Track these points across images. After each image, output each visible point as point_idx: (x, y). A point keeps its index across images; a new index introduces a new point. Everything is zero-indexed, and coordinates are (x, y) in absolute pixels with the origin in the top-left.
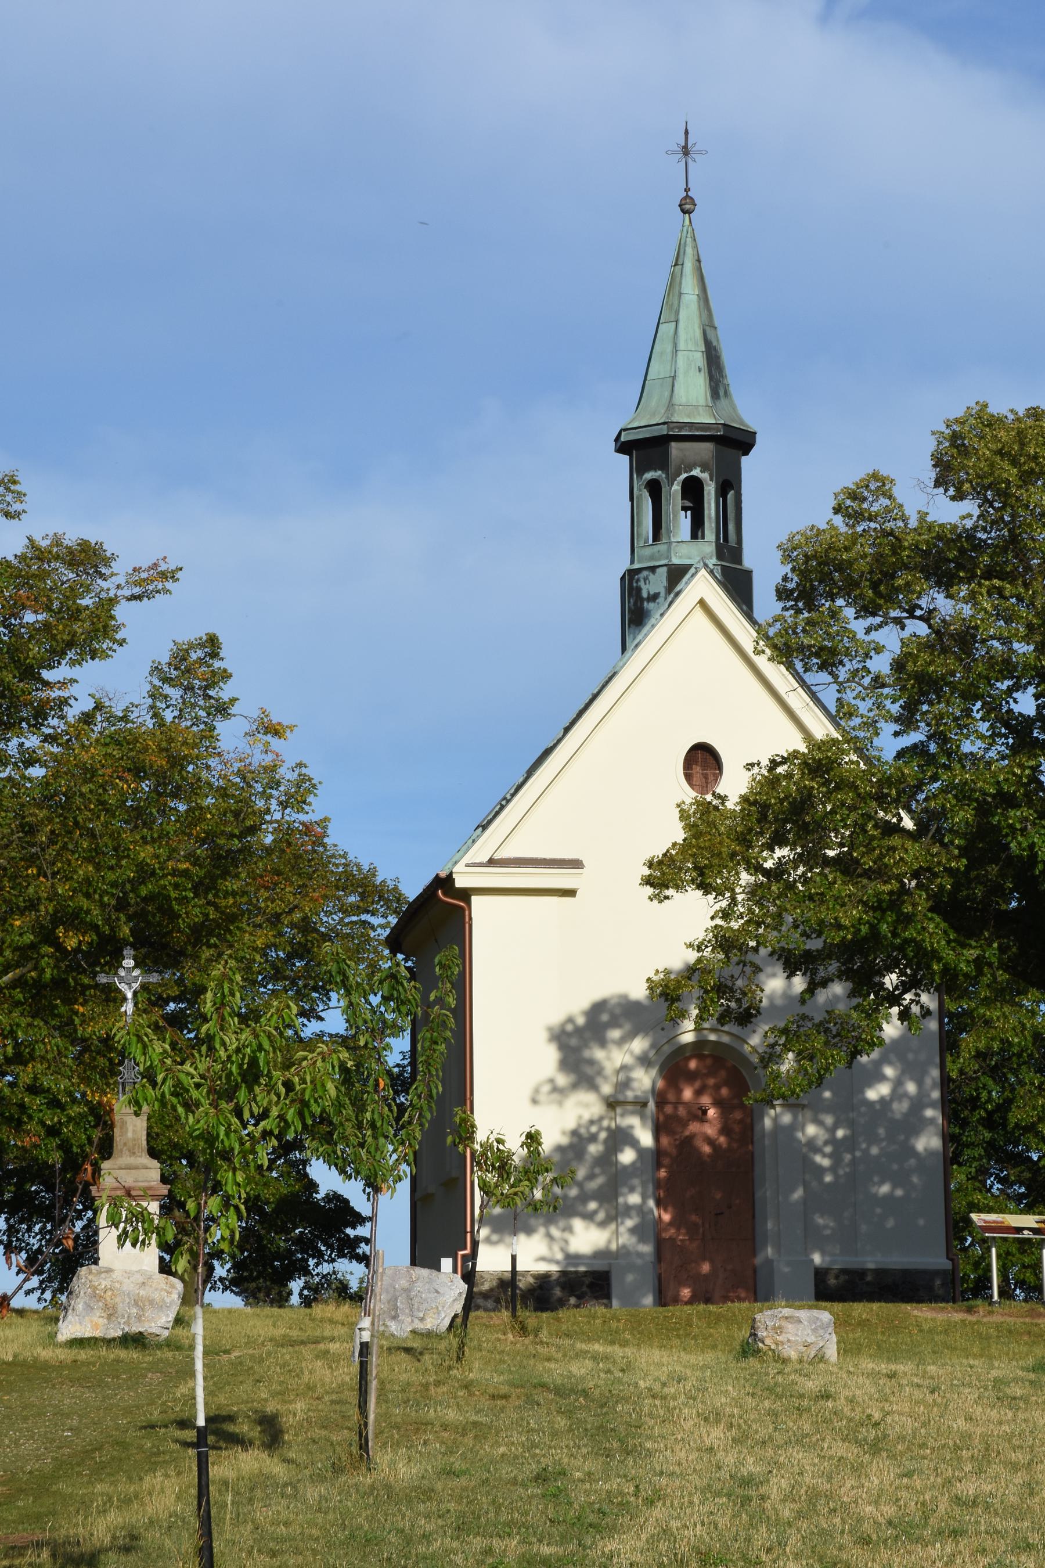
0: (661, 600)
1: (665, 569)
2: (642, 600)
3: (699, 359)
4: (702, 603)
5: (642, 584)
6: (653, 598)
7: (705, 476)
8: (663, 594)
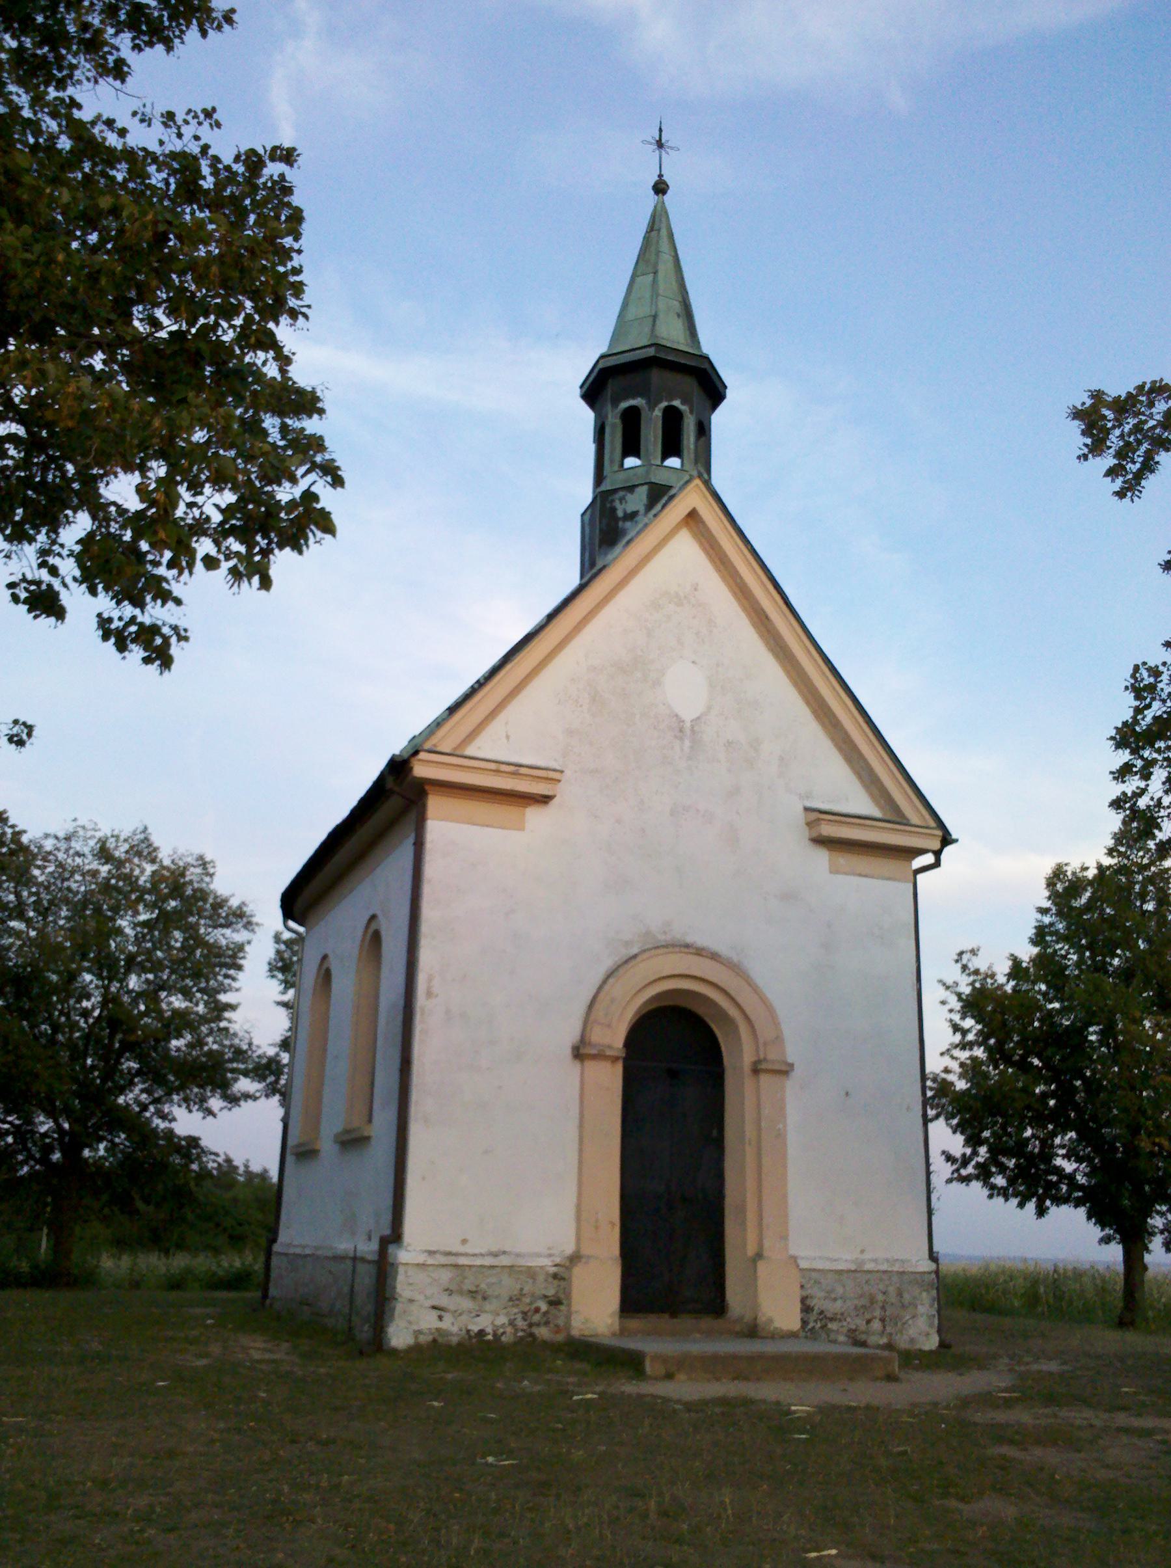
0: (638, 518)
1: (645, 488)
2: (617, 519)
3: (677, 306)
4: (693, 516)
5: (617, 504)
8: (642, 509)
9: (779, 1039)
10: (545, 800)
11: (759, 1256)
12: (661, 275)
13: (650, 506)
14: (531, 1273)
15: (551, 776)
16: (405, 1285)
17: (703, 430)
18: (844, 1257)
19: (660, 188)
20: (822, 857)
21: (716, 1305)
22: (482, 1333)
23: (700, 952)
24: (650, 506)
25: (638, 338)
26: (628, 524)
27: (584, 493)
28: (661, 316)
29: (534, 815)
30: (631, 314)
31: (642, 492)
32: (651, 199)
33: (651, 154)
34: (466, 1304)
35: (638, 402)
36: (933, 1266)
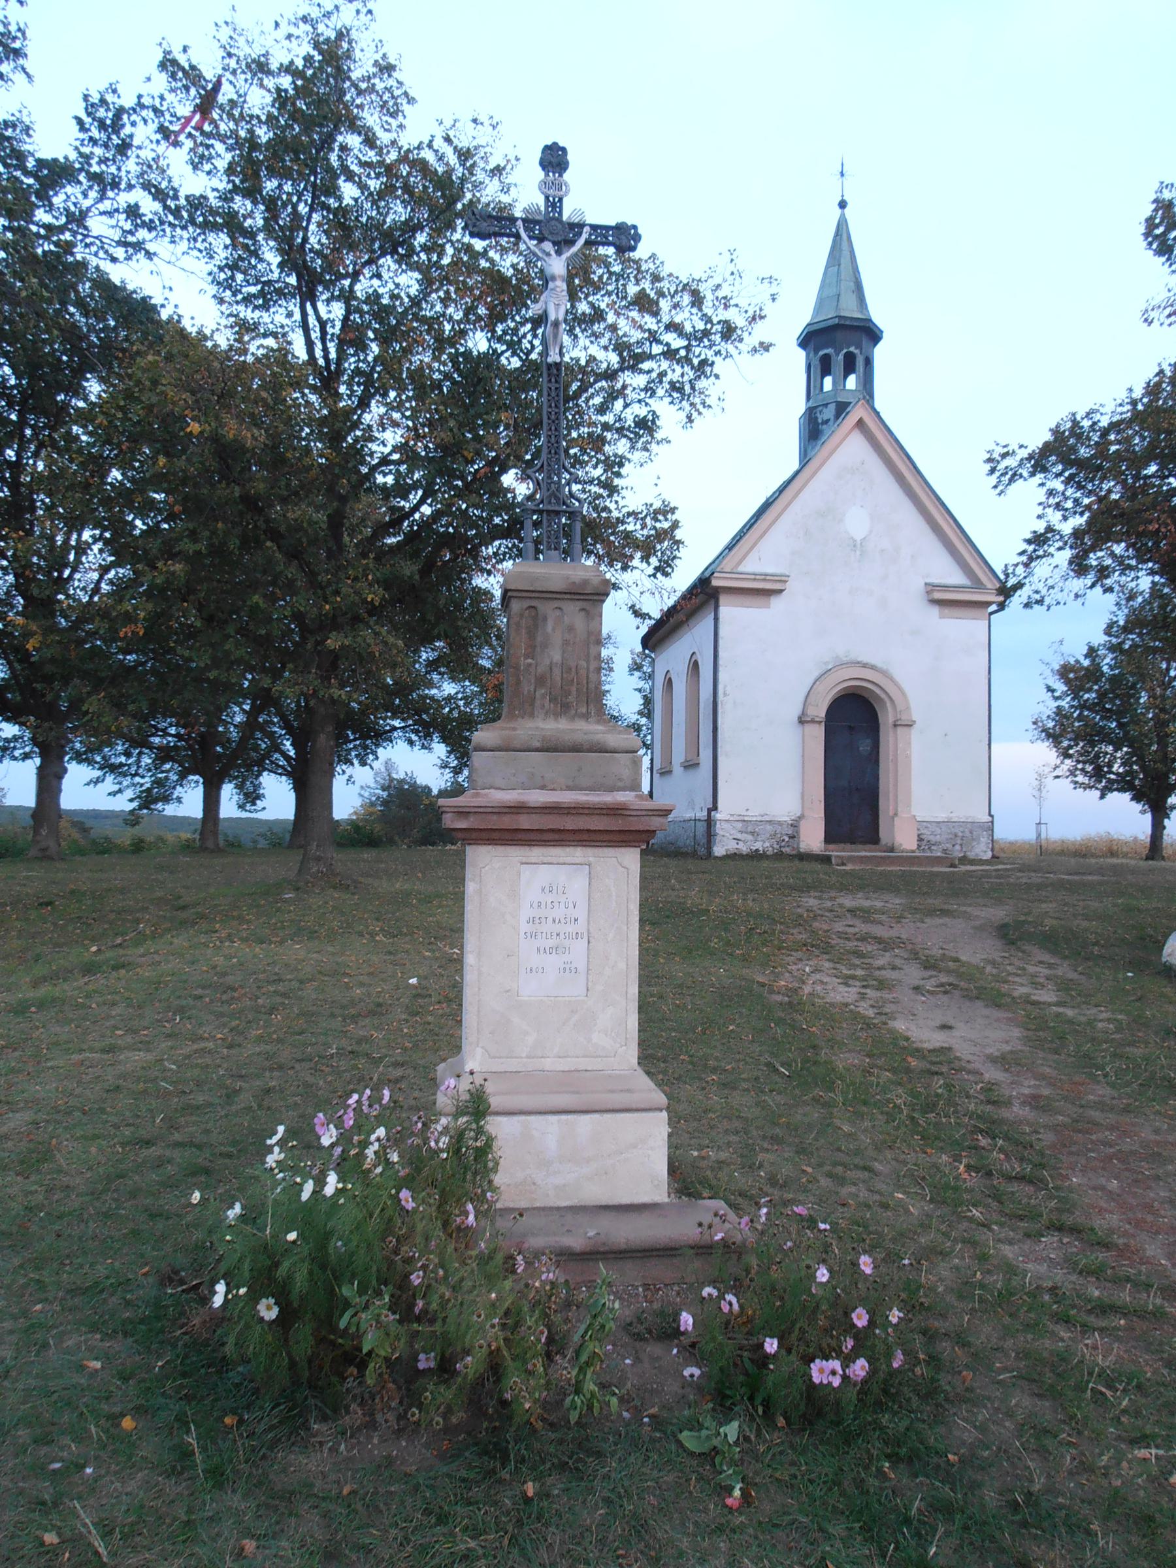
0: (831, 423)
6: (826, 422)
7: (857, 351)
9: (908, 708)
10: (781, 591)
11: (896, 814)
12: (842, 266)
13: (837, 416)
14: (780, 823)
15: (783, 579)
16: (719, 829)
17: (869, 362)
18: (942, 816)
19: (843, 205)
20: (935, 611)
21: (873, 838)
22: (757, 850)
23: (865, 666)
24: (837, 416)
25: (829, 313)
26: (824, 427)
27: (801, 407)
28: (842, 293)
29: (775, 601)
31: (832, 407)
32: (839, 211)
34: (750, 837)
35: (829, 351)
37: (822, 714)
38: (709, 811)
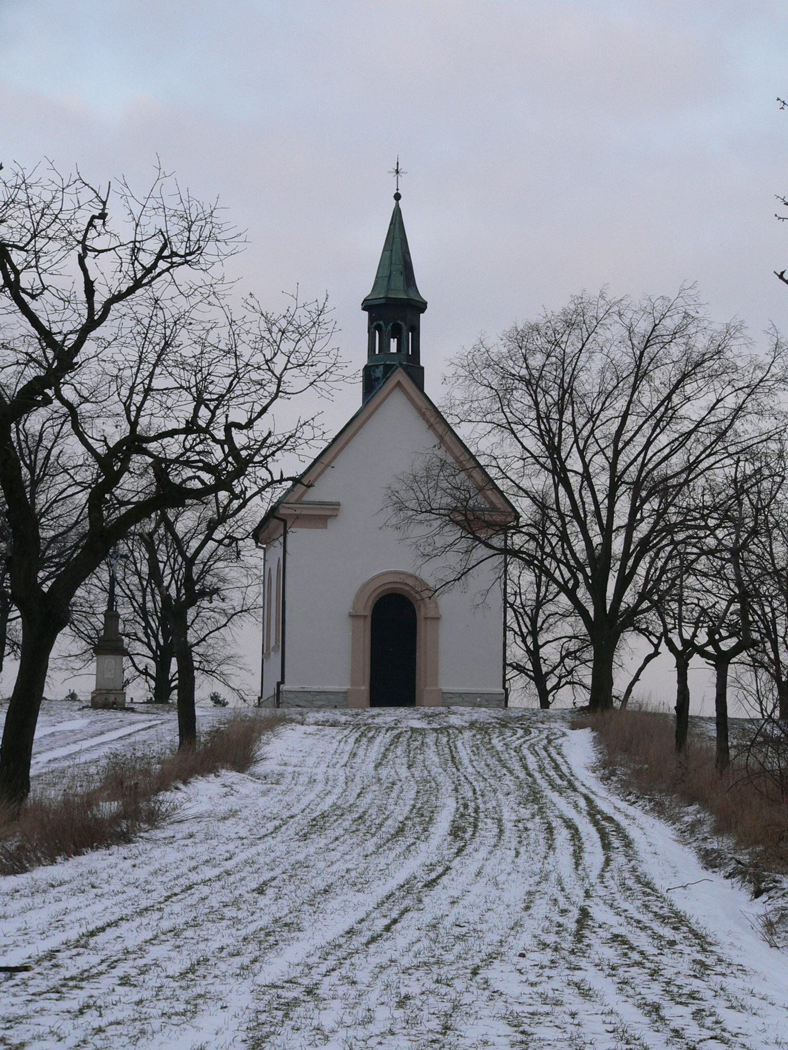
4: (399, 384)
13: (383, 378)
19: (397, 197)
30: (380, 275)
31: (381, 368)
33: (392, 177)
35: (381, 323)
36: (503, 691)
37: (368, 612)
38: (279, 684)
